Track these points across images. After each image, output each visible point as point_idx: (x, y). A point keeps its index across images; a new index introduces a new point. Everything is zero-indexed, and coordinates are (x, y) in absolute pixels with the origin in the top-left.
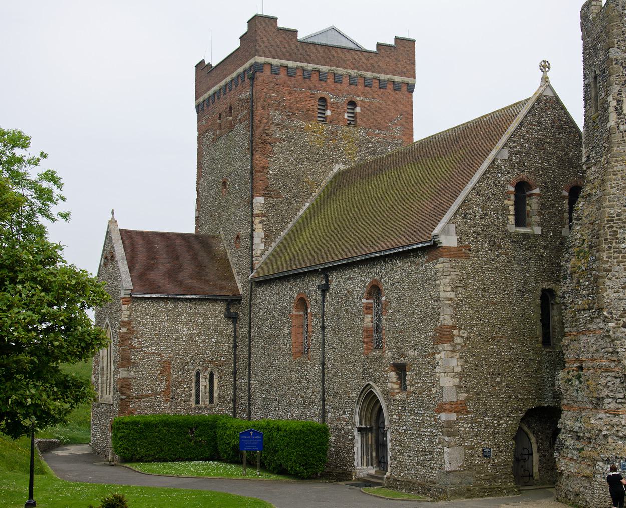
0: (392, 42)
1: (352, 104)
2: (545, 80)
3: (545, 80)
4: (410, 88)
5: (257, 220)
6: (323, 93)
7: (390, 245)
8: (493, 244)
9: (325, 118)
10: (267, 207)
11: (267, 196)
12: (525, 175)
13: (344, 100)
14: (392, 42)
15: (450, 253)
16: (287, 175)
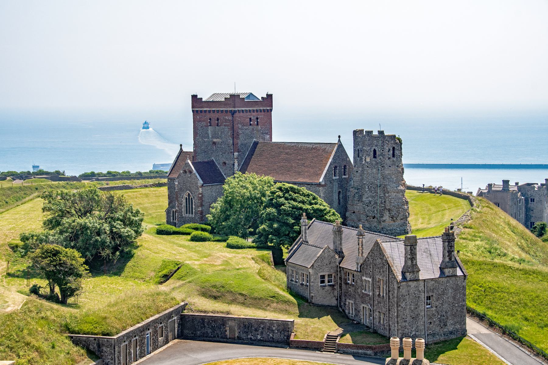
0: (265, 96)
1: (257, 119)
2: (339, 140)
3: (339, 140)
4: (271, 110)
5: (236, 160)
6: (249, 117)
7: (302, 181)
8: (331, 183)
9: (251, 125)
10: (239, 155)
11: (238, 152)
12: (336, 165)
13: (255, 118)
14: (265, 96)
15: (323, 186)
16: (242, 144)
